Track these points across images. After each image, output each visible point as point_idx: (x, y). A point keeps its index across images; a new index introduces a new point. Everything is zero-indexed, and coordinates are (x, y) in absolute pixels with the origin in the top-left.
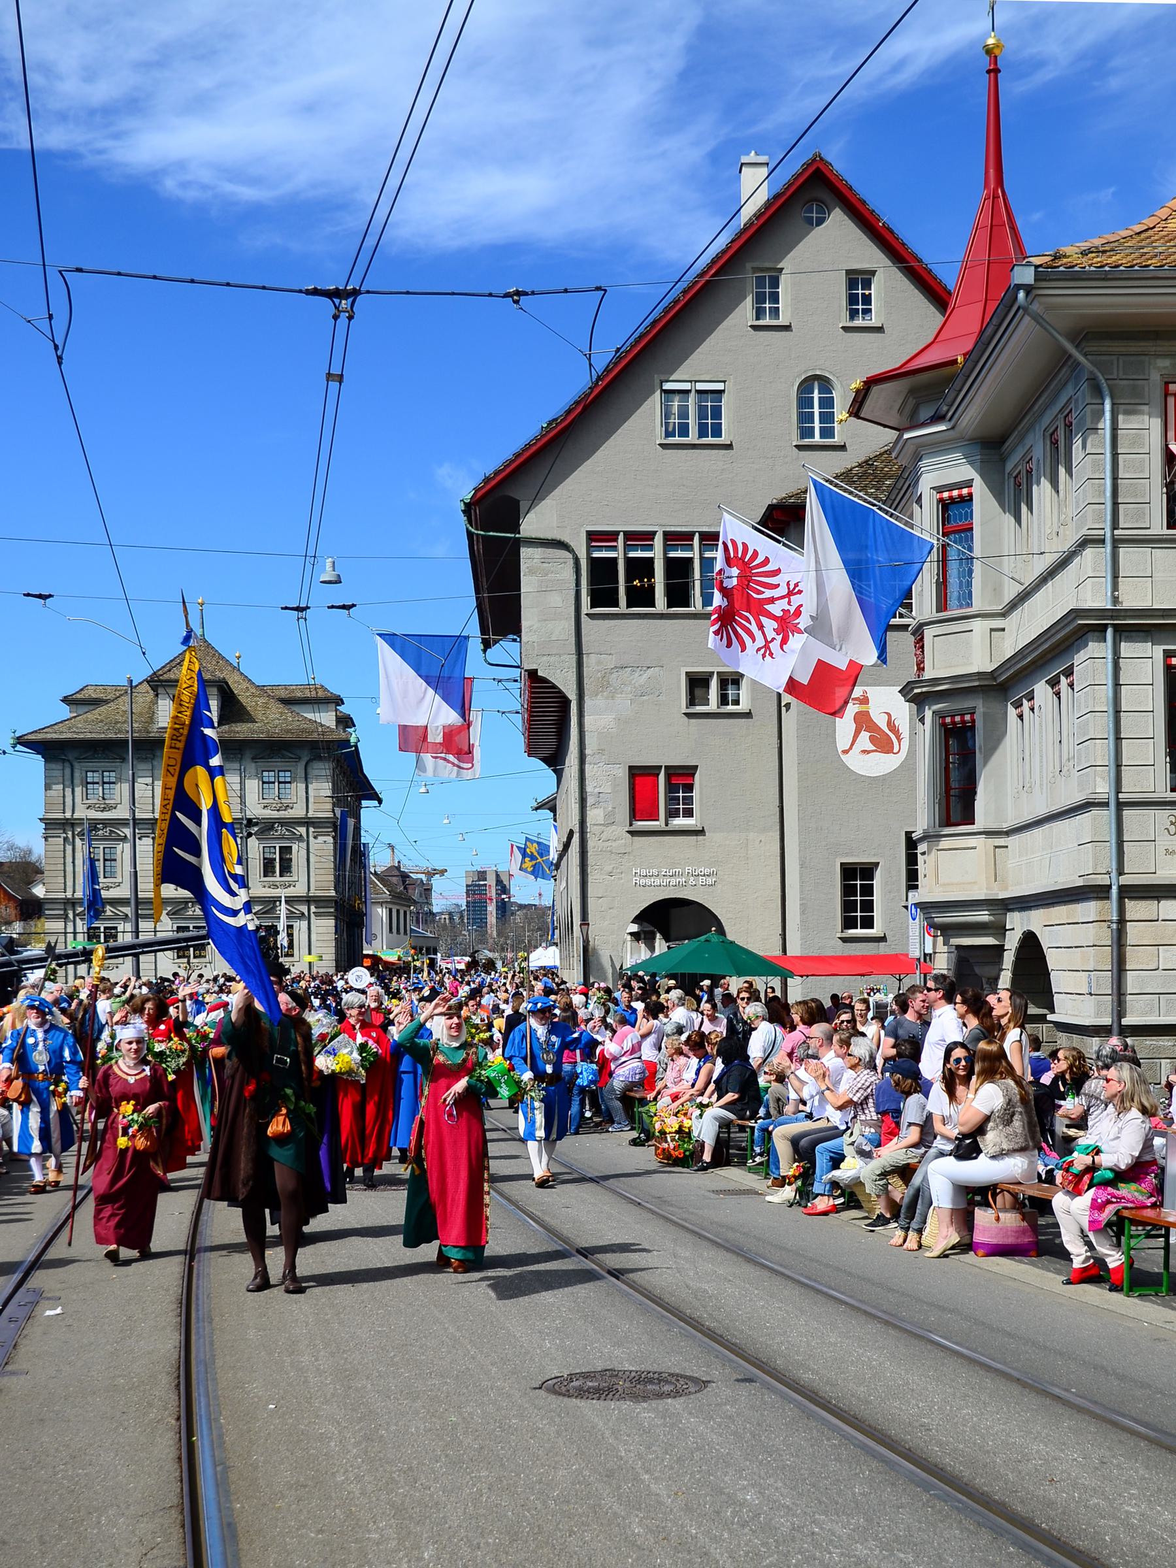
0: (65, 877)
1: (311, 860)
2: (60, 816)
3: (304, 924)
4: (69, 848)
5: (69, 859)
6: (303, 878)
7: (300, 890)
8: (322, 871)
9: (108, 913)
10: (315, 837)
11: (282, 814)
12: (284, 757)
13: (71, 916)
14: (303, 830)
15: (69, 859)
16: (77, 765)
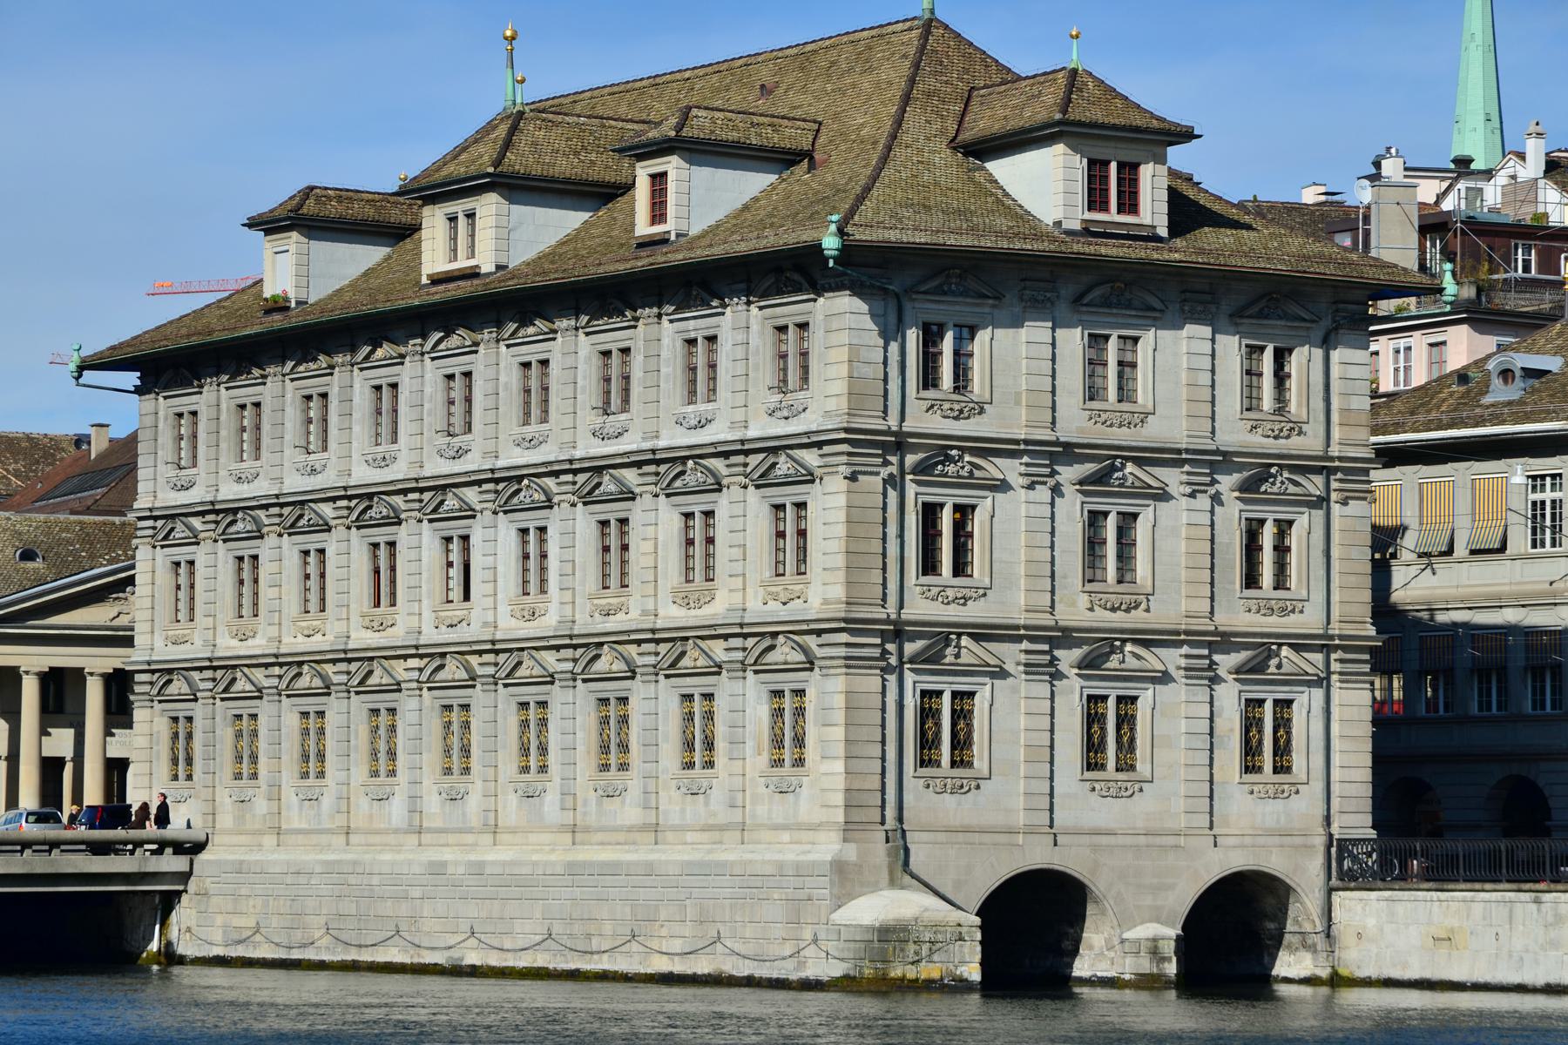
0: (884, 569)
1: (1335, 552)
2: (879, 425)
3: (1318, 694)
4: (893, 495)
5: (892, 530)
6: (1318, 596)
7: (1308, 621)
8: (1353, 579)
9: (966, 658)
10: (1344, 503)
11: (1282, 446)
12: (1285, 316)
13: (893, 661)
14: (1314, 485)
15: (892, 530)
16: (908, 306)
